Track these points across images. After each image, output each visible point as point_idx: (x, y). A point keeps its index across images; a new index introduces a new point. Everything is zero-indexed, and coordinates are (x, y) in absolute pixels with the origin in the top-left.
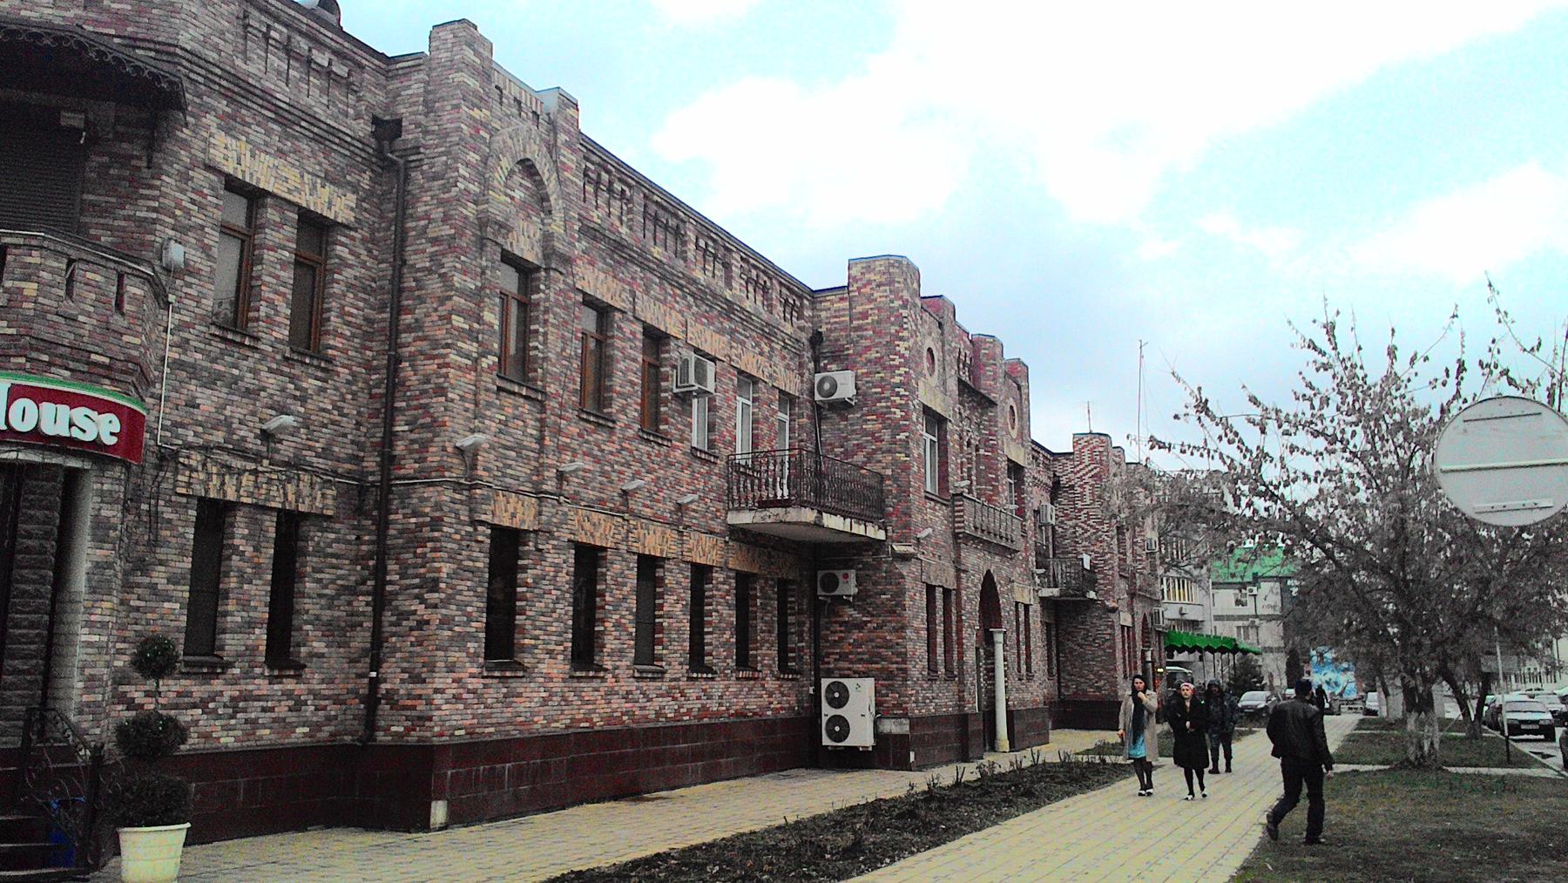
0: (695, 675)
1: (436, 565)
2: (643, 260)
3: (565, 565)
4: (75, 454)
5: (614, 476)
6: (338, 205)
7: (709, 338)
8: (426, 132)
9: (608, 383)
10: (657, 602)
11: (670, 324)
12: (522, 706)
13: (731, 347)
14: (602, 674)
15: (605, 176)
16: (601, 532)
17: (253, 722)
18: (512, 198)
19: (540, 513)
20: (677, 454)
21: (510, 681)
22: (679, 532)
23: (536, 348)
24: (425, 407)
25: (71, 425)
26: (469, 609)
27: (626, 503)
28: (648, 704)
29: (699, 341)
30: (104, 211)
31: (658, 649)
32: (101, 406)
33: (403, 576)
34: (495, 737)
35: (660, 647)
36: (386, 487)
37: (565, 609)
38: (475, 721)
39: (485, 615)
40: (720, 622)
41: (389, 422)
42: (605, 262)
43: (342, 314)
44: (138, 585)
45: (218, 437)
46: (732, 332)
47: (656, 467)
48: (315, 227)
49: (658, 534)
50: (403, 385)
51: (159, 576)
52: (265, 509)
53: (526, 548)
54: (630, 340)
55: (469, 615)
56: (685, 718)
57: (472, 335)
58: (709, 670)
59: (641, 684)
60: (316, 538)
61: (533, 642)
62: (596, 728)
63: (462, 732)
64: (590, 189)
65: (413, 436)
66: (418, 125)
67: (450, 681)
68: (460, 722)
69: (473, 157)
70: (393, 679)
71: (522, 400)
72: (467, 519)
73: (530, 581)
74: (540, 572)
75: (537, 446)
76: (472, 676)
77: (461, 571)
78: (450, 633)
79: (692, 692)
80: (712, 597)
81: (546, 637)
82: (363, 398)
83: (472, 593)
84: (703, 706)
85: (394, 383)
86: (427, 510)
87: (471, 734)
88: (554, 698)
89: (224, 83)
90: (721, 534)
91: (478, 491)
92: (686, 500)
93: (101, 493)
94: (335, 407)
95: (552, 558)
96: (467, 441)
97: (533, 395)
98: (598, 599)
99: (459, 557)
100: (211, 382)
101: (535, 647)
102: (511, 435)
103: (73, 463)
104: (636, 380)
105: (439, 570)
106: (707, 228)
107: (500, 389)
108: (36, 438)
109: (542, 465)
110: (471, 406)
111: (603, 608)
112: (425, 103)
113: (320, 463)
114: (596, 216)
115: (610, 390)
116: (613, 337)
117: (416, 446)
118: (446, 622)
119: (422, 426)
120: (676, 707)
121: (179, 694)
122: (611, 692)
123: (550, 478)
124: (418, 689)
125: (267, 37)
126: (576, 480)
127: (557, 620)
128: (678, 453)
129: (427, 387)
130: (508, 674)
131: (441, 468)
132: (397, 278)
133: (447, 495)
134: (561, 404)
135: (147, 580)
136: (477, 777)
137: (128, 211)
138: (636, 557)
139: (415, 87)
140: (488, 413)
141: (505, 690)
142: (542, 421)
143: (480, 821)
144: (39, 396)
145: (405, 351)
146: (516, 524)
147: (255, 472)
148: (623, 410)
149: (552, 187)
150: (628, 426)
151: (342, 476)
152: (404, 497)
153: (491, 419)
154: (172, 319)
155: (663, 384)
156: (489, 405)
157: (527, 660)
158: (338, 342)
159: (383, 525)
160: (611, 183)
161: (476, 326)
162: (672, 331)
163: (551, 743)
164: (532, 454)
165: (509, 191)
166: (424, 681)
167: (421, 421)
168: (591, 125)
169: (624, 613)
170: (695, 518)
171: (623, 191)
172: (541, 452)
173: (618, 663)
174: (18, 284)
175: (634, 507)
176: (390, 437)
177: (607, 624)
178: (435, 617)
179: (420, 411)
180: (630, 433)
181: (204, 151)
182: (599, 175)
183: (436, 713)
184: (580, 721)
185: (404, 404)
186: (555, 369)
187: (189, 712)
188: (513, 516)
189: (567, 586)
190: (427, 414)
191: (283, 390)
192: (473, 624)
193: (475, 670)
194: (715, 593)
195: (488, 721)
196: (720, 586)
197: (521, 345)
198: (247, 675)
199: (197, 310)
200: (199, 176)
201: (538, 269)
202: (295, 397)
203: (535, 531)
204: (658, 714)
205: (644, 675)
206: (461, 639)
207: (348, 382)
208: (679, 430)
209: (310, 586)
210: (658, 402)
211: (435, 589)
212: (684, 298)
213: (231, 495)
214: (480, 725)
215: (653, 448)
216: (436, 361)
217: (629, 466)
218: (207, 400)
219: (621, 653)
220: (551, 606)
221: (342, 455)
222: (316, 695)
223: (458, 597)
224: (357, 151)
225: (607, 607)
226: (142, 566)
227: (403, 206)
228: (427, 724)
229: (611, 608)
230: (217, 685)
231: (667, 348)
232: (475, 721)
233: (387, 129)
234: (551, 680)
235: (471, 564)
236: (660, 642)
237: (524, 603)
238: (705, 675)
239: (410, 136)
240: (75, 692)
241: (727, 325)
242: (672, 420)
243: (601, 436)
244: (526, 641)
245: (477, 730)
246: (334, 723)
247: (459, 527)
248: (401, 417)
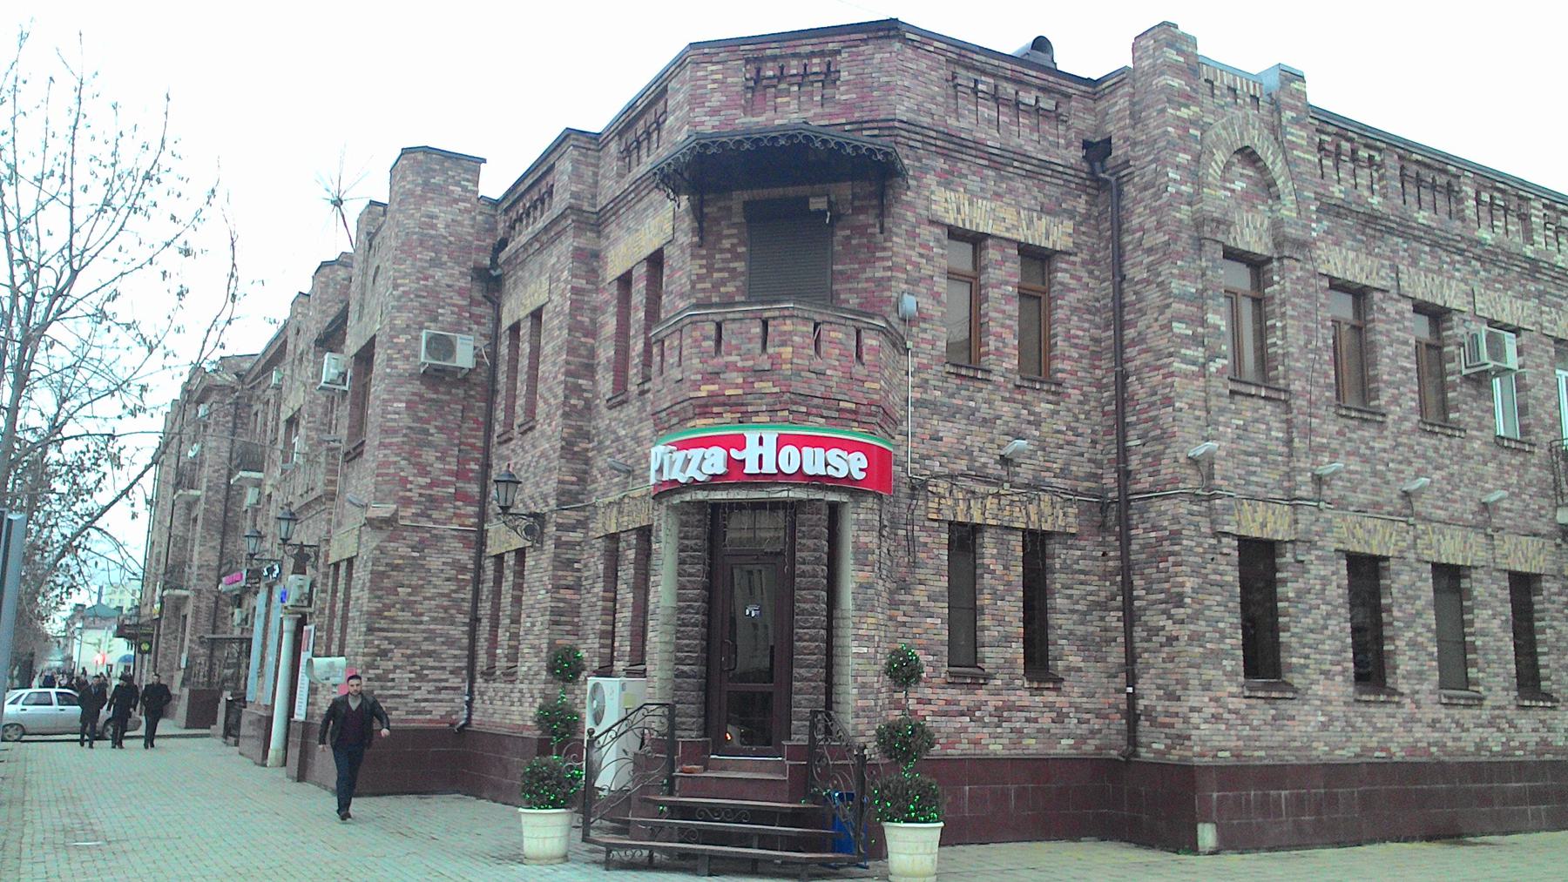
0: (1527, 703)
1: (1180, 579)
2: (1405, 230)
3: (1334, 577)
4: (833, 489)
5: (1390, 476)
6: (1054, 233)
7: (1507, 306)
8: (1134, 144)
9: (1371, 373)
10: (1466, 617)
11: (1451, 296)
12: (1296, 729)
13: (1542, 313)
14: (1396, 699)
15: (1346, 146)
16: (1378, 539)
17: (1020, 731)
18: (1233, 191)
19: (1296, 522)
20: (1476, 446)
21: (1279, 702)
22: (1486, 535)
23: (1275, 344)
24: (1154, 419)
25: (827, 464)
26: (1221, 625)
27: (1410, 505)
28: (1464, 734)
29: (1492, 310)
30: (849, 278)
31: (1473, 673)
32: (850, 447)
33: (1149, 591)
34: (1266, 762)
35: (1475, 670)
36: (1125, 502)
37: (1340, 627)
38: (1241, 743)
39: (1240, 631)
40: (1557, 641)
41: (1122, 438)
42: (1355, 239)
43: (1068, 337)
44: (903, 602)
45: (962, 465)
46: (1540, 295)
47: (1448, 462)
48: (1036, 258)
49: (1458, 539)
50: (1133, 399)
51: (920, 594)
52: (1010, 529)
53: (1284, 560)
54: (1396, 321)
55: (1222, 632)
56: (1517, 753)
57: (1197, 341)
58: (1548, 696)
59: (1451, 711)
60: (1060, 555)
61: (1302, 661)
62: (1395, 759)
63: (1227, 754)
64: (1328, 162)
65: (1146, 450)
66: (1126, 139)
67: (1206, 699)
68: (1223, 744)
69: (1183, 158)
70: (1149, 697)
71: (1262, 402)
72: (1208, 531)
73: (1291, 595)
74: (1302, 586)
75: (1285, 450)
76: (1232, 695)
77: (1207, 584)
78: (1201, 650)
79: (1525, 722)
80: (1543, 611)
81: (1318, 656)
82: (1096, 417)
83: (1222, 608)
84: (1544, 740)
85: (1122, 400)
86: (1166, 523)
87: (1237, 756)
88: (1336, 723)
89: (939, 143)
90: (1549, 536)
91: (1217, 501)
92: (1492, 498)
93: (858, 522)
94: (1069, 428)
95: (1317, 569)
96: (1199, 450)
97: (1274, 395)
98: (1384, 615)
99: (1203, 571)
100: (950, 417)
101: (1307, 666)
102: (1253, 440)
103: (832, 497)
104: (1408, 366)
105: (1182, 585)
106: (1488, 179)
107: (1233, 393)
108: (801, 478)
109: (1293, 469)
110: (1203, 414)
111: (1391, 624)
112: (1132, 115)
113: (1059, 483)
114: (1337, 191)
115: (1375, 379)
116: (1373, 320)
117: (1150, 460)
118: (1195, 638)
119: (1155, 439)
120: (1504, 740)
121: (948, 702)
122: (1412, 719)
123: (1305, 483)
124: (1174, 707)
125: (975, 91)
126: (1340, 483)
127: (1330, 638)
128: (1477, 445)
129: (1154, 398)
130: (1274, 695)
131: (1175, 481)
132: (1119, 293)
133: (1184, 508)
134: (1310, 402)
135: (910, 598)
136: (1248, 801)
137: (869, 274)
138: (1430, 566)
139: (1121, 102)
140: (1221, 419)
141: (1273, 712)
142: (1288, 421)
143: (1258, 849)
144: (801, 442)
145: (1131, 366)
146: (1267, 534)
147: (997, 495)
148: (1395, 400)
149: (1277, 168)
150: (1402, 419)
151: (1082, 494)
152: (1142, 511)
153: (1227, 425)
154: (911, 363)
155: (1448, 366)
156: (1222, 411)
157: (1297, 680)
158: (1067, 366)
159: (1125, 540)
160: (1354, 151)
161: (1200, 330)
162: (1454, 304)
163: (1335, 772)
164: (1280, 458)
165: (1228, 185)
166: (1179, 699)
167: (1152, 434)
168: (1319, 95)
169: (1419, 630)
170: (1510, 519)
171: (1371, 158)
172: (1290, 455)
173: (1417, 687)
174: (777, 349)
175: (1420, 509)
176: (1124, 453)
177: (1398, 643)
178: (1184, 632)
179: (1150, 424)
180: (1407, 425)
181: (927, 209)
182: (1338, 146)
183: (1194, 732)
184: (1376, 749)
185: (1134, 419)
186: (1299, 365)
187: (958, 719)
188: (1263, 525)
189: (1341, 601)
190: (1156, 427)
191: (1017, 416)
192: (1228, 641)
193: (1234, 689)
194: (1547, 605)
195: (1257, 744)
196: (1555, 598)
197: (1259, 344)
198: (1009, 686)
199: (933, 352)
200: (926, 232)
201: (1269, 260)
202: (1029, 422)
203: (1291, 542)
204: (1479, 747)
205: (1455, 701)
206: (1216, 657)
207: (1080, 402)
208: (1475, 417)
209: (1060, 602)
210: (1443, 388)
211: (1181, 604)
212: (1467, 263)
213: (977, 519)
214: (1247, 747)
215: (1441, 440)
216: (1161, 372)
217: (1410, 463)
218: (949, 432)
219: (1420, 676)
220: (1322, 622)
221: (1081, 474)
222: (1077, 709)
223: (1207, 613)
224: (1071, 178)
225: (1396, 623)
226: (904, 585)
227: (1118, 227)
228: (1186, 743)
229: (1402, 625)
230: (982, 694)
231: (1449, 324)
232: (1241, 743)
233: (1097, 150)
234: (1330, 702)
235: (1218, 577)
236: (1475, 664)
237: (1287, 619)
238: (1541, 704)
239: (1119, 152)
240: (850, 696)
241: (1532, 287)
242: (1464, 407)
243: (1368, 432)
244: (1294, 660)
245: (1244, 753)
246: (1098, 736)
247: (1200, 540)
248: (1132, 432)
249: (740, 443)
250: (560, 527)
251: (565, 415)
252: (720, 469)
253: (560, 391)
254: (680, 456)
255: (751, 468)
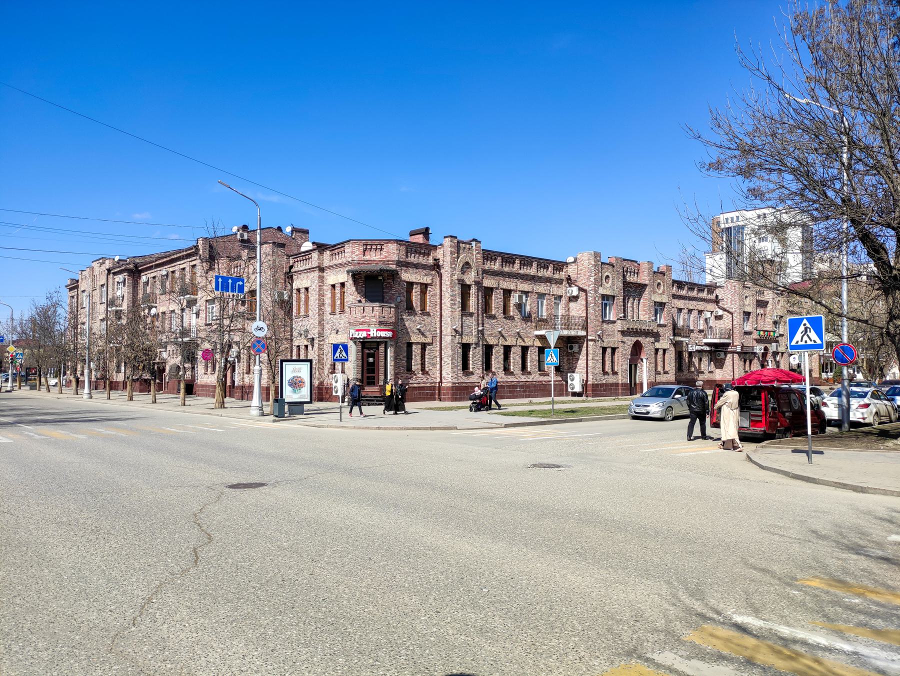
30: (387, 293)
51: (401, 357)
108: (380, 337)
144: (380, 330)
146: (467, 342)
249: (369, 330)
250: (319, 341)
251: (319, 315)
252: (366, 336)
253: (317, 310)
254: (357, 333)
255: (372, 335)
